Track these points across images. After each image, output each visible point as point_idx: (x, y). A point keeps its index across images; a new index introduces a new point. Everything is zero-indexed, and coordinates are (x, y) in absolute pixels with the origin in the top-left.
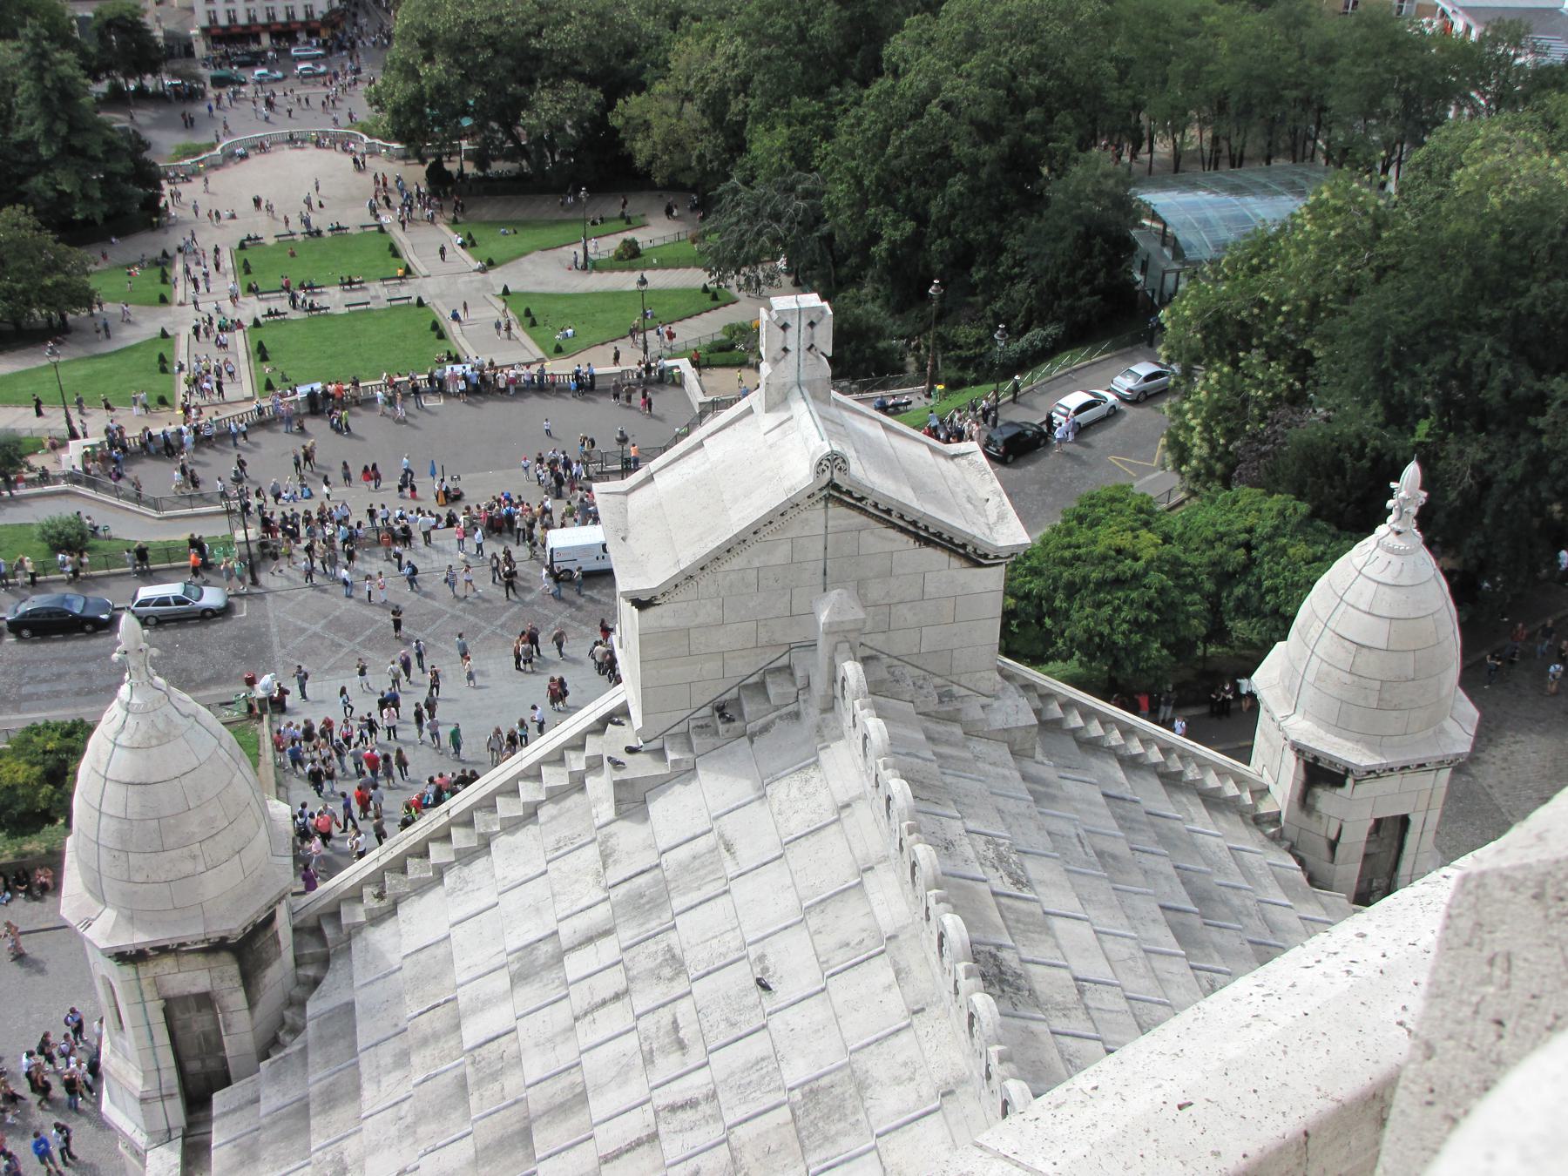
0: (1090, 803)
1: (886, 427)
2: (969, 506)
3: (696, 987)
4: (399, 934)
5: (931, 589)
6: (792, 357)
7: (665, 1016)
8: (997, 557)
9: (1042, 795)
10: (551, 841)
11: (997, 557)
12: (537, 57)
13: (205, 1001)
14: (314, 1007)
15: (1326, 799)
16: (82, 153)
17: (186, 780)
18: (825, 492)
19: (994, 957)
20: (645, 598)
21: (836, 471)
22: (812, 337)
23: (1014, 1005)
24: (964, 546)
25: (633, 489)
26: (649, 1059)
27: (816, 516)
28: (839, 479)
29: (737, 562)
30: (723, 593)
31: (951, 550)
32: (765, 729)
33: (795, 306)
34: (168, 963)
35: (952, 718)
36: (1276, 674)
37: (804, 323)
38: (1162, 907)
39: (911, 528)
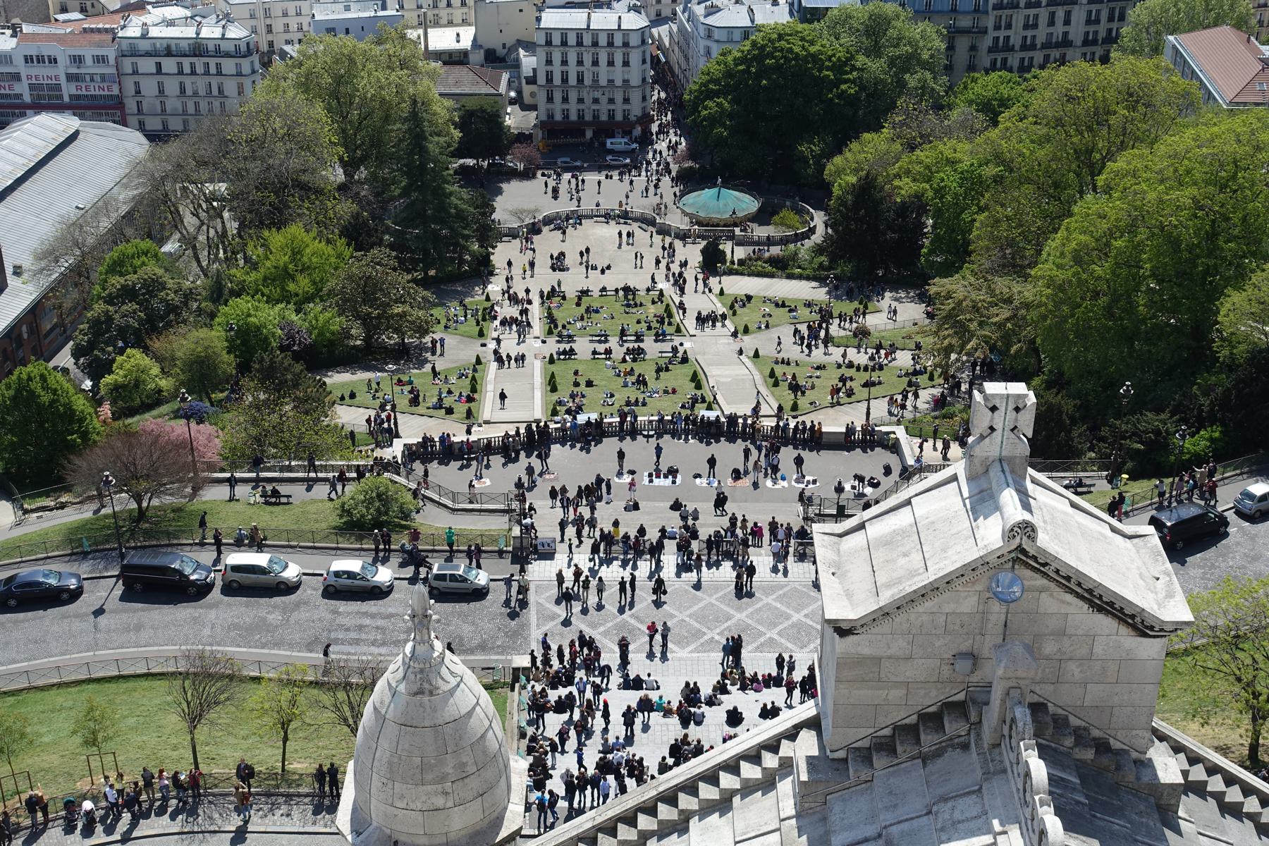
1: (1074, 505)
2: (1141, 582)
5: (1098, 650)
6: (997, 435)
8: (1162, 630)
11: (1162, 630)
18: (1013, 555)
20: (845, 626)
21: (1025, 538)
22: (1016, 420)
24: (1133, 617)
29: (928, 605)
30: (914, 631)
31: (1120, 619)
33: (1005, 392)
37: (1011, 406)
39: (1086, 595)
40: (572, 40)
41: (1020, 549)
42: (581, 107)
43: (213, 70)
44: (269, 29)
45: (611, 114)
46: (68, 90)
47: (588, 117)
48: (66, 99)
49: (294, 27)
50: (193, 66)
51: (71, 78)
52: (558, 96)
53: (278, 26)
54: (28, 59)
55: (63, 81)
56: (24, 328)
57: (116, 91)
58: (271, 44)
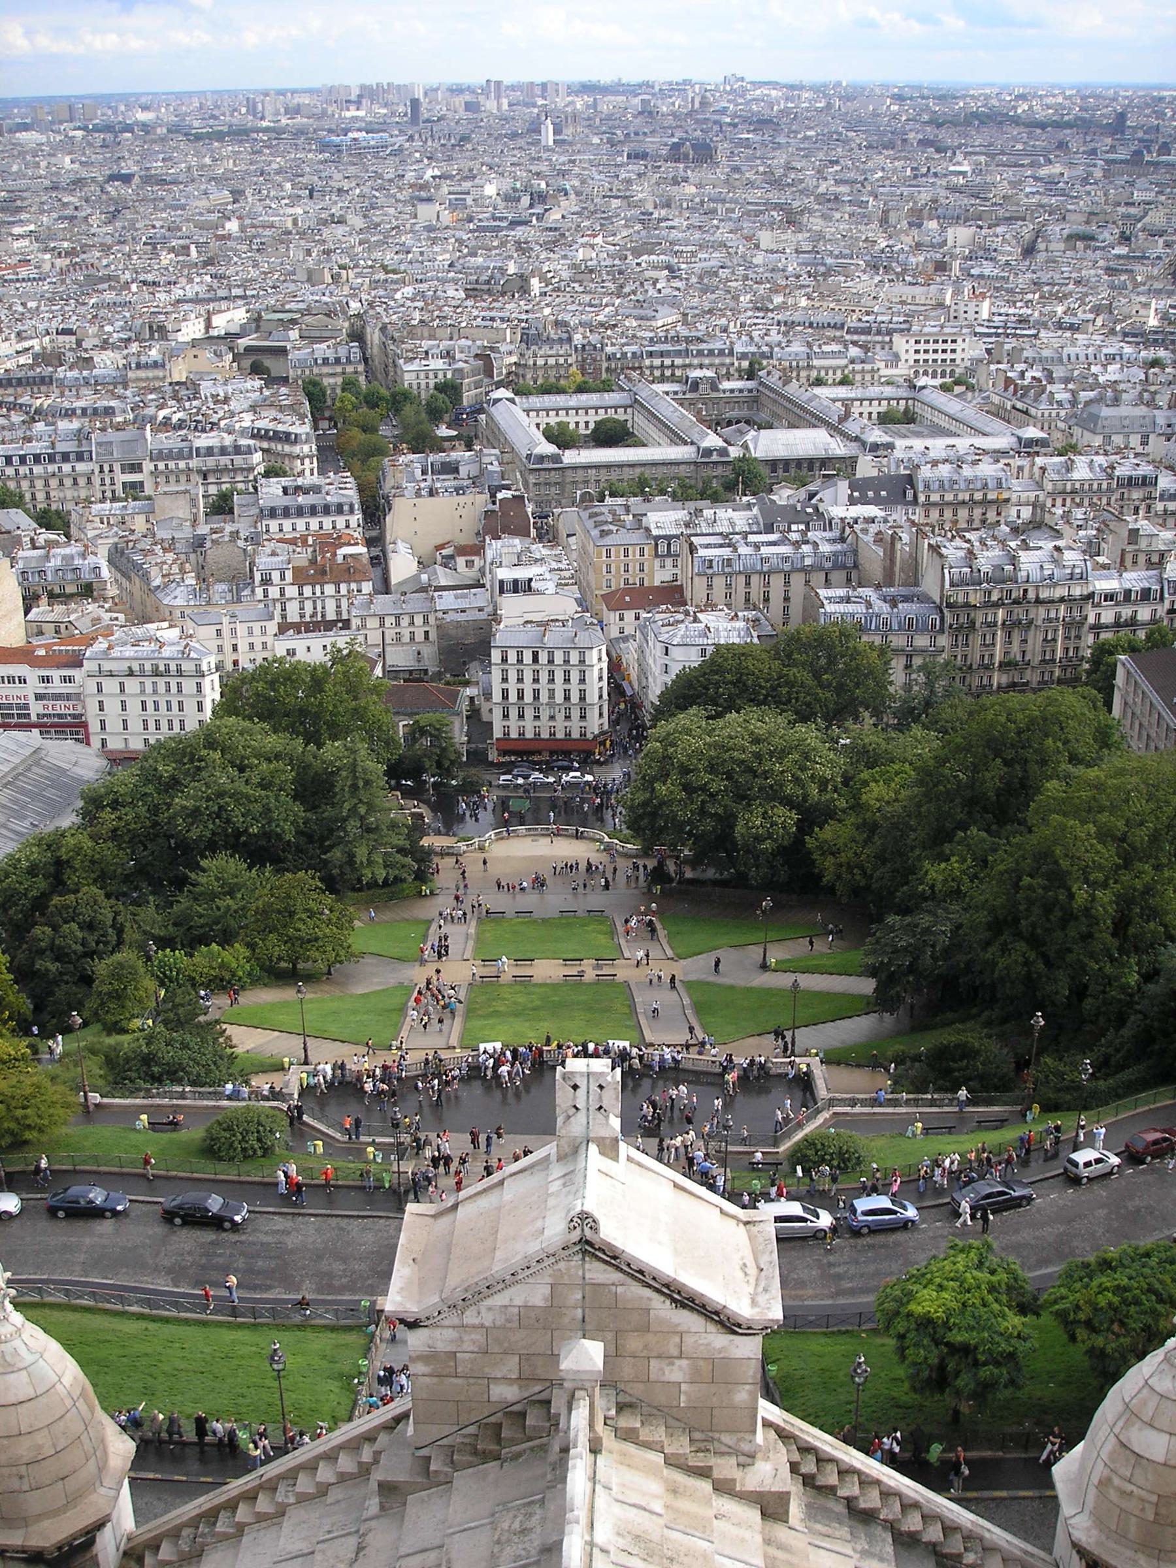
6: (581, 1116)
18: (578, 1248)
21: (587, 1229)
22: (600, 1098)
24: (717, 1313)
35: (703, 1473)
37: (594, 1087)
40: (528, 657)
41: (584, 1241)
42: (537, 723)
43: (174, 689)
44: (235, 648)
46: (36, 709)
49: (258, 647)
51: (39, 697)
52: (513, 713)
53: (243, 647)
55: (31, 700)
57: (79, 711)
58: (236, 663)
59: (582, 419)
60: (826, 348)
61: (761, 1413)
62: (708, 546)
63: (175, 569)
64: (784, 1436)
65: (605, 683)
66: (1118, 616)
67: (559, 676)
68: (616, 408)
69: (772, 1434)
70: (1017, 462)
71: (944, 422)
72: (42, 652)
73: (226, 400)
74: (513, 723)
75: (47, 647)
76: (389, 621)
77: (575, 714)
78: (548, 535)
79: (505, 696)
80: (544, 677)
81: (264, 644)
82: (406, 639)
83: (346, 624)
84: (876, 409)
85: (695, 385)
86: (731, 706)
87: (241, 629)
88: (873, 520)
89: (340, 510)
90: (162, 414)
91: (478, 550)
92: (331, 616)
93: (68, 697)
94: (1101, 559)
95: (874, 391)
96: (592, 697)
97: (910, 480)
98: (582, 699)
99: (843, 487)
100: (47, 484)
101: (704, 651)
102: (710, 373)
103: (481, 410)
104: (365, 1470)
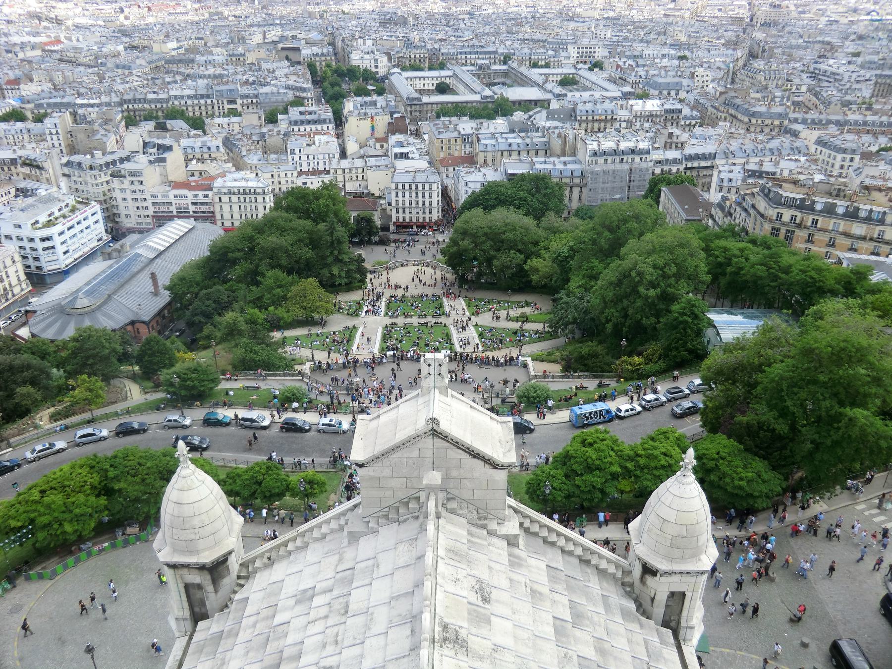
0: (539, 569)
3: (348, 620)
4: (270, 574)
5: (477, 475)
6: (432, 377)
7: (336, 629)
9: (515, 563)
10: (326, 549)
12: (502, 242)
13: (199, 587)
14: (237, 597)
15: (650, 580)
16: (341, 261)
17: (195, 505)
19: (457, 631)
23: (456, 654)
25: (373, 419)
26: (324, 646)
27: (429, 441)
28: (435, 427)
29: (398, 454)
32: (405, 521)
34: (185, 571)
35: (484, 527)
36: (638, 525)
38: (554, 617)
44: (280, 182)
45: (424, 218)
46: (192, 209)
47: (414, 220)
48: (191, 213)
49: (290, 182)
50: (245, 199)
51: (193, 204)
52: (401, 211)
53: (283, 182)
54: (175, 196)
56: (166, 312)
57: (212, 210)
58: (280, 189)
59: (431, 82)
60: (538, 51)
61: (508, 502)
62: (486, 138)
63: (252, 147)
64: (516, 511)
65: (440, 198)
66: (662, 170)
67: (420, 195)
68: (445, 77)
69: (512, 511)
70: (620, 103)
71: (589, 85)
72: (194, 184)
73: (274, 71)
74: (401, 215)
75: (196, 181)
76: (347, 171)
77: (427, 211)
78: (417, 133)
79: (397, 204)
80: (414, 195)
81: (292, 181)
82: (354, 178)
83: (328, 172)
84: (559, 78)
85: (480, 67)
86: (494, 207)
87: (283, 174)
88: (556, 128)
89: (324, 121)
90: (245, 77)
91: (385, 140)
92: (321, 168)
93: (206, 204)
94: (655, 146)
95: (560, 71)
96: (435, 204)
97: (574, 110)
98: (430, 204)
99: (544, 113)
100: (194, 109)
101: (482, 184)
102: (487, 62)
103: (387, 78)
104: (341, 528)
